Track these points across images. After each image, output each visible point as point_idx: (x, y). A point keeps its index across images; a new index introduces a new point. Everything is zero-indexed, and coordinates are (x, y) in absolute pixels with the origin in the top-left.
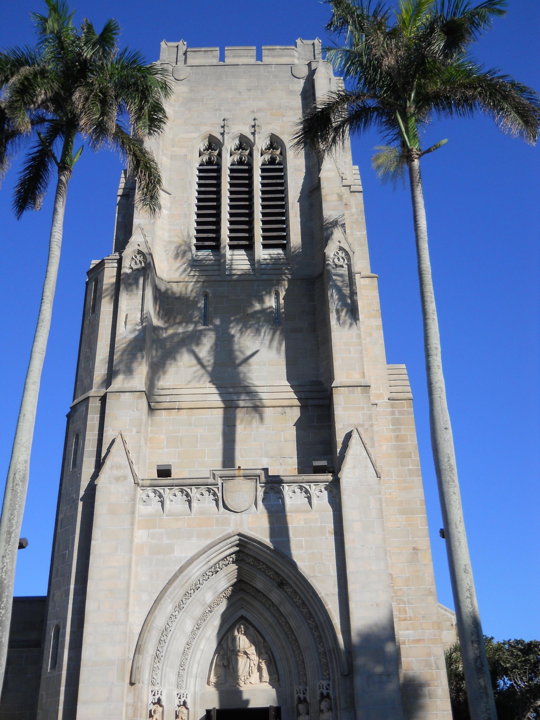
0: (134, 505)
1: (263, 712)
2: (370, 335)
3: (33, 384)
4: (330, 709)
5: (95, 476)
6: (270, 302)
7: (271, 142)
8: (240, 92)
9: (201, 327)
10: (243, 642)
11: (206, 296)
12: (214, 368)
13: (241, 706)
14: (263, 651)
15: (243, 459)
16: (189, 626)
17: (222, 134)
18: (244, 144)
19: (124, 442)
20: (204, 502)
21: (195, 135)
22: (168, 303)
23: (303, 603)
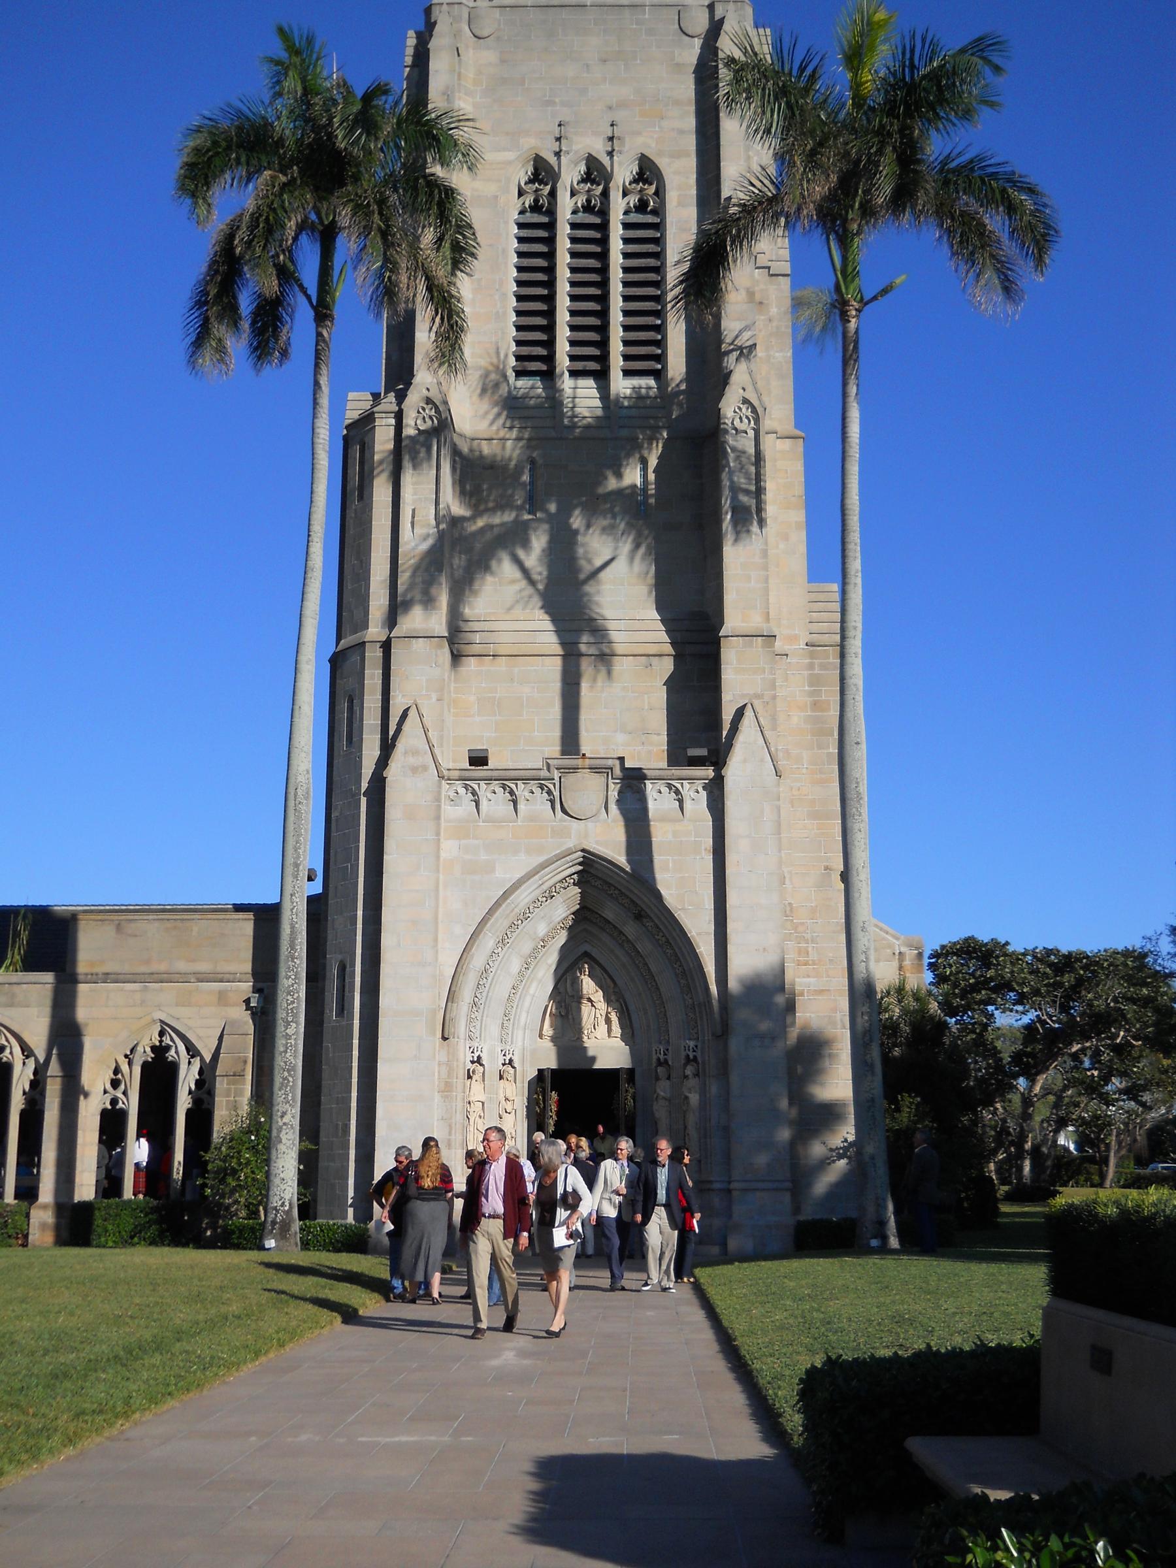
0: (439, 807)
1: (611, 1075)
2: (786, 538)
3: (307, 663)
4: (697, 1075)
5: (383, 762)
6: (633, 476)
7: (641, 168)
8: (588, 66)
9: (527, 517)
10: (588, 985)
11: (533, 462)
12: (547, 586)
13: (583, 1066)
14: (613, 998)
15: (589, 744)
16: (515, 965)
17: (558, 154)
18: (595, 173)
19: (421, 716)
20: (535, 803)
21: (510, 155)
22: (476, 474)
23: (668, 941)
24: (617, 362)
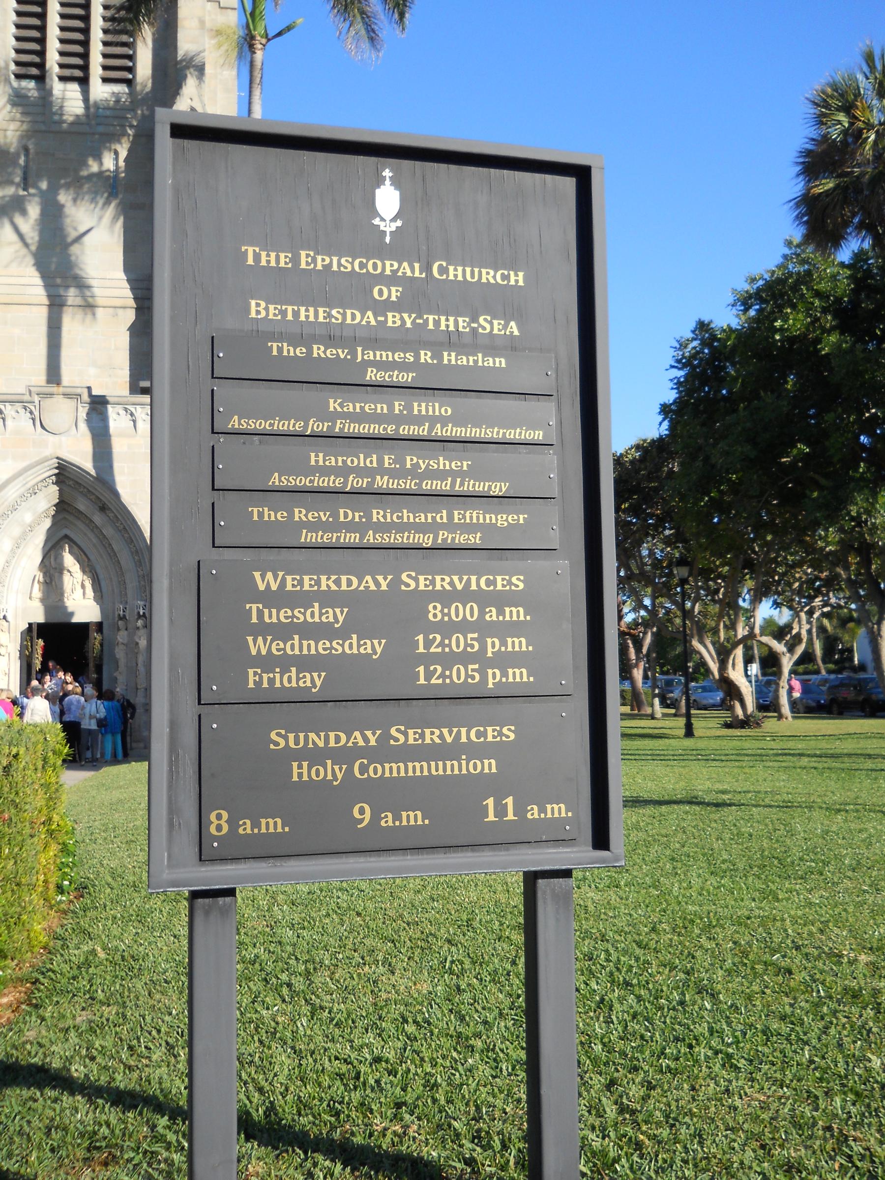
1: (84, 628)
6: (108, 163)
9: (22, 193)
10: (69, 560)
11: (26, 150)
12: (38, 248)
14: (87, 569)
23: (124, 528)
24: (96, 71)
